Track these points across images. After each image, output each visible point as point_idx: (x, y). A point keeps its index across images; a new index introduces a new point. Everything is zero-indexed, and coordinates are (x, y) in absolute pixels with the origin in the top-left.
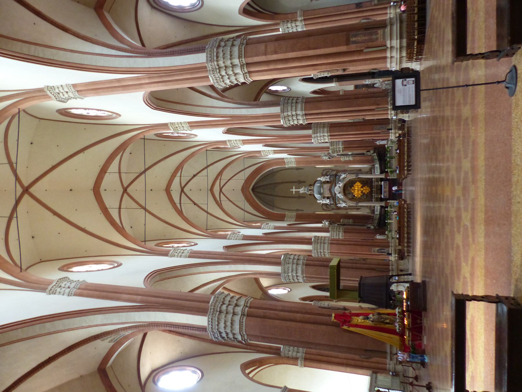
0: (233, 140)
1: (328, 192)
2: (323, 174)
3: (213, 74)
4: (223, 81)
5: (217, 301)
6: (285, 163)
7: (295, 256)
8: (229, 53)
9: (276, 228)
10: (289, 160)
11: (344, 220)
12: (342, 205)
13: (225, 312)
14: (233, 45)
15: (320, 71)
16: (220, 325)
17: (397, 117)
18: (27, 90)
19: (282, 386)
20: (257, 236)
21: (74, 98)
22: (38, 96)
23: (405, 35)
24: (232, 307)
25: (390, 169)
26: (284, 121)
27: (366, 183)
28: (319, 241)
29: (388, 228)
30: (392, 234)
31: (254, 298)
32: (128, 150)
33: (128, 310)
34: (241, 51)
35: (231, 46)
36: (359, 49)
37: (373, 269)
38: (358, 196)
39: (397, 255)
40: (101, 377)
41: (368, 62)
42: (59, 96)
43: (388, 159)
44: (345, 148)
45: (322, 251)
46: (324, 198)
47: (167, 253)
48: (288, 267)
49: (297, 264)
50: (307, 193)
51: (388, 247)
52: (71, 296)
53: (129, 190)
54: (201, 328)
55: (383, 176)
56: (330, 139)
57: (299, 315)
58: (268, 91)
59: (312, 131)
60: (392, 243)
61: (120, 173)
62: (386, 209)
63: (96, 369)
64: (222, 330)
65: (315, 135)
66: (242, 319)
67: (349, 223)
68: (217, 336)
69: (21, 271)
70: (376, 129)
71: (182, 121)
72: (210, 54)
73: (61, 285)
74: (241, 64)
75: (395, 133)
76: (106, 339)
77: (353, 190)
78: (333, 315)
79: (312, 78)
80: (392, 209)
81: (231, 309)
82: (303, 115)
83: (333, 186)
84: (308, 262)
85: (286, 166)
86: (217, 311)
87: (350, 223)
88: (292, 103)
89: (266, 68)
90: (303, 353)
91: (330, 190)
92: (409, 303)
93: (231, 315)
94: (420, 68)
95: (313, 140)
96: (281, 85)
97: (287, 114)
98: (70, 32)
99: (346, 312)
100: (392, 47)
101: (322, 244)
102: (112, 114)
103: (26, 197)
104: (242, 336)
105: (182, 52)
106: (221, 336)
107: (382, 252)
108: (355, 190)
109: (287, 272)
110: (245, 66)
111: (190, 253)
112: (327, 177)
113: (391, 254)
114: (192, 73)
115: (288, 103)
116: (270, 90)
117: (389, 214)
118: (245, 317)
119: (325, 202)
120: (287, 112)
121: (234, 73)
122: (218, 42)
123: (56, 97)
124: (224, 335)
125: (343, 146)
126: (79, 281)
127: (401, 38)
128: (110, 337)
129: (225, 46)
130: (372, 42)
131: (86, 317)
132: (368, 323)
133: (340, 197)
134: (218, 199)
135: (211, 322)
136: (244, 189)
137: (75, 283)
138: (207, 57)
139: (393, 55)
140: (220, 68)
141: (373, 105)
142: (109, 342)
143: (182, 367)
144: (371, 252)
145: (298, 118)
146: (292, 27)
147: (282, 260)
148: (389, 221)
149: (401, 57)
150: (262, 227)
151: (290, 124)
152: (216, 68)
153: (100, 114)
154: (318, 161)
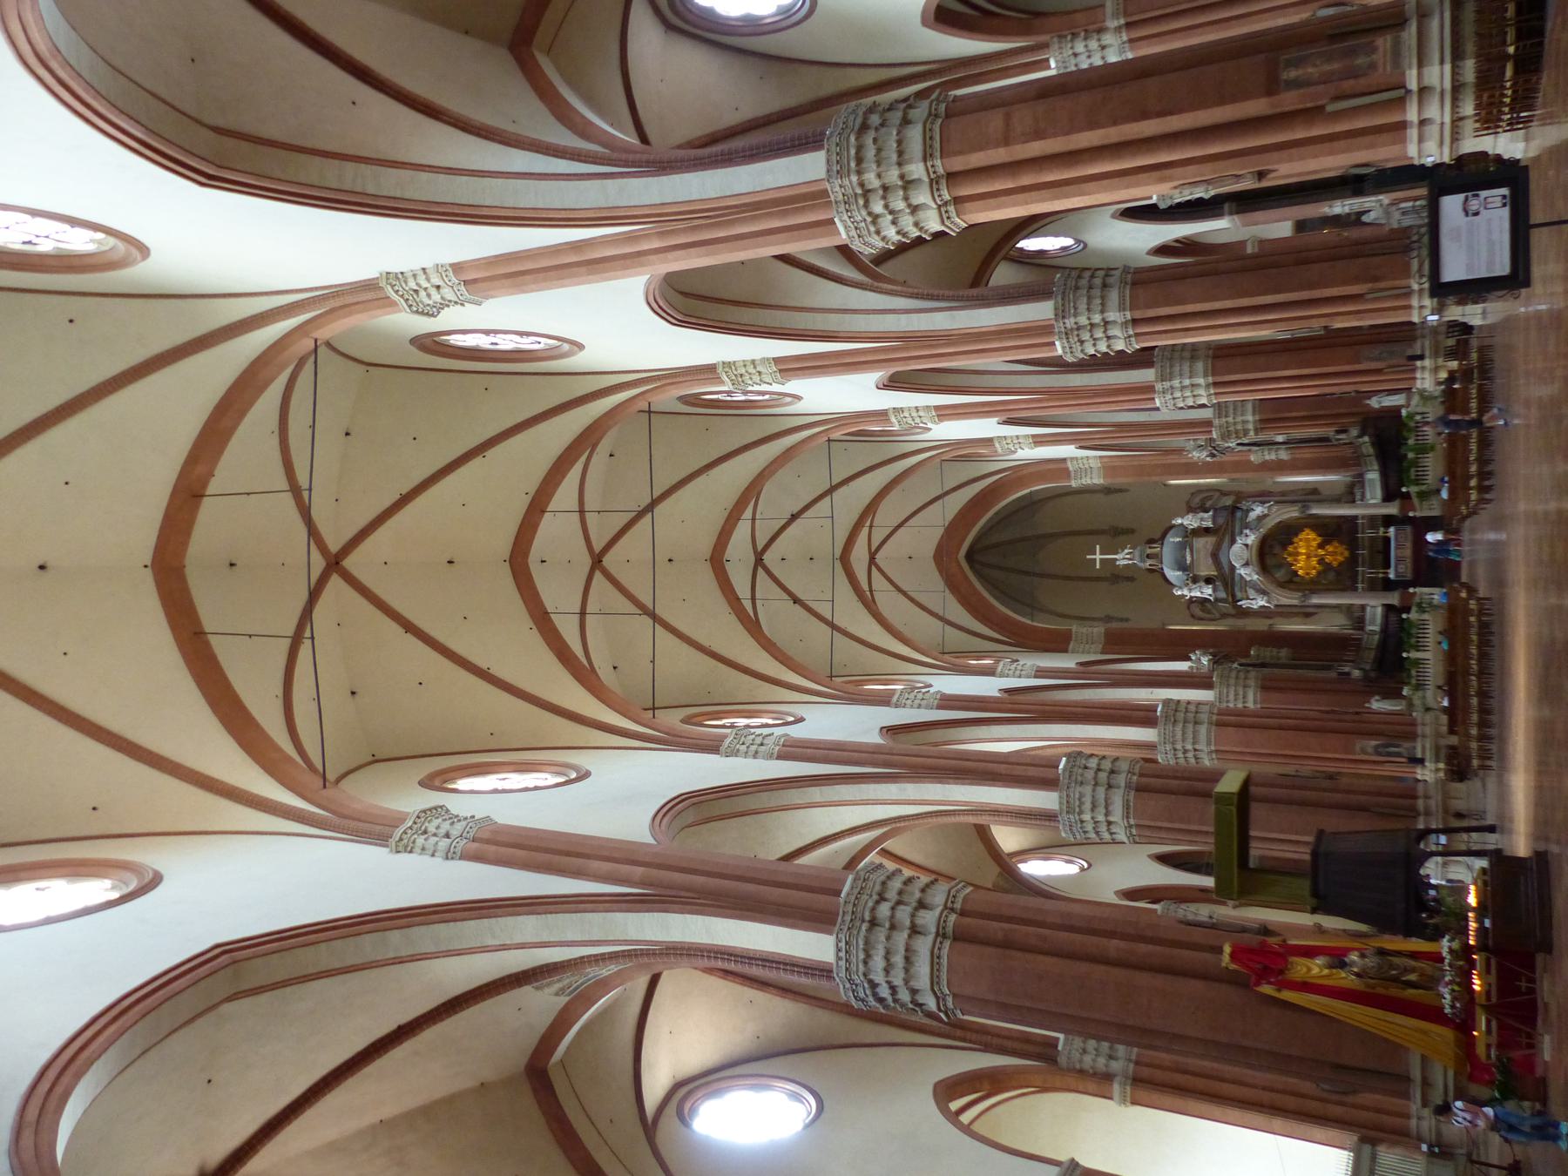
0: (909, 409)
1: (1210, 561)
2: (1193, 505)
3: (847, 211)
4: (878, 232)
5: (862, 888)
7: (1103, 762)
8: (895, 145)
9: (1040, 673)
10: (1081, 465)
11: (1262, 649)
12: (1253, 602)
13: (887, 925)
14: (906, 122)
15: (1181, 182)
16: (871, 963)
17: (1441, 317)
18: (336, 286)
19: (1063, 1157)
20: (984, 697)
21: (456, 303)
22: (363, 302)
23: (1470, 47)
24: (909, 909)
25: (1417, 484)
26: (1066, 345)
27: (1331, 531)
28: (1181, 716)
29: (1409, 676)
30: (1424, 697)
31: (976, 886)
32: (604, 447)
33: (607, 905)
34: (931, 138)
35: (901, 125)
36: (1309, 105)
37: (1362, 809)
39: (1442, 765)
40: (535, 1091)
41: (1342, 144)
42: (418, 300)
43: (1411, 455)
44: (1260, 420)
45: (1189, 747)
46: (1195, 580)
47: (716, 743)
48: (1081, 796)
49: (1110, 786)
50: (1141, 565)
51: (1412, 737)
52: (452, 858)
53: (607, 561)
54: (816, 969)
55: (1392, 509)
56: (1216, 394)
57: (1115, 942)
58: (1016, 254)
59: (1157, 372)
61: (582, 512)
62: (1404, 616)
63: (522, 1068)
64: (879, 977)
65: (1167, 384)
66: (939, 949)
67: (1279, 659)
68: (862, 995)
69: (325, 787)
71: (757, 356)
72: (838, 154)
73: (426, 827)
74: (933, 176)
75: (1436, 369)
76: (549, 985)
77: (1290, 555)
78: (1227, 949)
79: (1154, 206)
80: (1426, 616)
81: (904, 914)
82: (1125, 324)
84: (1145, 780)
85: (1074, 484)
86: (863, 921)
87: (1284, 661)
88: (1091, 288)
89: (1010, 185)
90: (1130, 1060)
91: (1215, 556)
92: (1487, 923)
93: (905, 934)
94: (1526, 151)
95: (1157, 401)
96: (1056, 235)
97: (1076, 323)
98: (445, 118)
99: (1272, 940)
100: (1423, 91)
101: (1190, 727)
102: (560, 343)
103: (335, 581)
104: (937, 998)
105: (754, 152)
106: (875, 995)
107: (1389, 754)
108: (1298, 554)
109: (1077, 810)
110: (944, 182)
111: (783, 746)
112: (1206, 515)
113: (1421, 761)
114: (785, 213)
115: (1077, 288)
116: (1021, 249)
117: (1414, 631)
118: (949, 942)
119: (1198, 594)
120: (1075, 315)
121: (909, 206)
122: (861, 113)
123: (410, 302)
124: (884, 992)
125: (1257, 417)
126: (473, 817)
127: (1457, 56)
128: (559, 981)
129: (882, 125)
130: (1356, 77)
131: (493, 920)
132: (1344, 979)
133: (1248, 579)
134: (865, 587)
135: (845, 951)
136: (942, 555)
137: (464, 823)
138: (828, 161)
139: (1426, 115)
140: (867, 193)
141: (1356, 280)
142: (557, 994)
143: (760, 1081)
144: (1355, 754)
145: (1110, 333)
146: (1089, 51)
147: (1060, 772)
148: (1414, 655)
149: (1457, 121)
150: (999, 669)
151: (1086, 354)
152: (856, 194)
153: (526, 344)
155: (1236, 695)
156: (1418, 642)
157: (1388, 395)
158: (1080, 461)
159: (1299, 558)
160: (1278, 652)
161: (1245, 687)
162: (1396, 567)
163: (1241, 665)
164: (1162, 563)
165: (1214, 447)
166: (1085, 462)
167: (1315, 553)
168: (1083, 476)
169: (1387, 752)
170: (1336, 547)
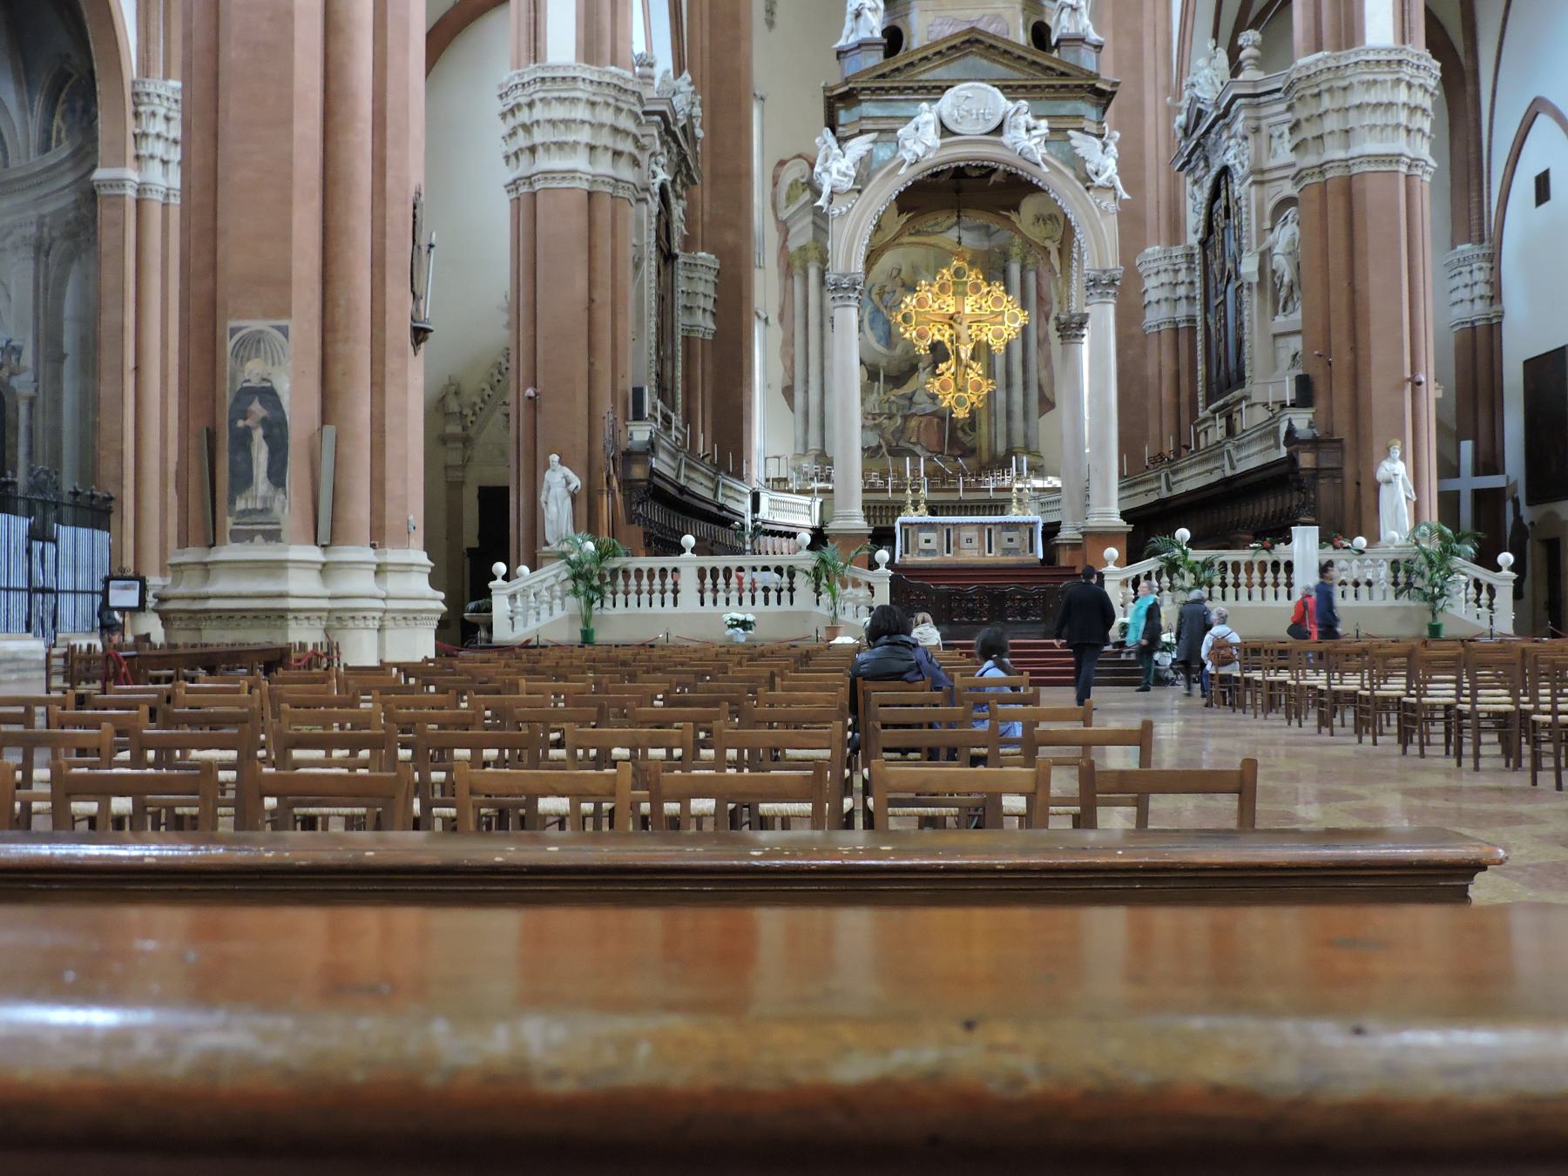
11: (711, 277)
38: (906, 318)
60: (380, 570)
67: (688, 309)
77: (958, 273)
83: (1000, 71)
87: (682, 319)
108: (960, 294)
155: (567, 122)
157: (1407, 498)
159: (950, 300)
161: (592, 148)
162: (930, 527)
165: (1225, 114)
167: (964, 336)
169: (247, 432)
170: (978, 387)
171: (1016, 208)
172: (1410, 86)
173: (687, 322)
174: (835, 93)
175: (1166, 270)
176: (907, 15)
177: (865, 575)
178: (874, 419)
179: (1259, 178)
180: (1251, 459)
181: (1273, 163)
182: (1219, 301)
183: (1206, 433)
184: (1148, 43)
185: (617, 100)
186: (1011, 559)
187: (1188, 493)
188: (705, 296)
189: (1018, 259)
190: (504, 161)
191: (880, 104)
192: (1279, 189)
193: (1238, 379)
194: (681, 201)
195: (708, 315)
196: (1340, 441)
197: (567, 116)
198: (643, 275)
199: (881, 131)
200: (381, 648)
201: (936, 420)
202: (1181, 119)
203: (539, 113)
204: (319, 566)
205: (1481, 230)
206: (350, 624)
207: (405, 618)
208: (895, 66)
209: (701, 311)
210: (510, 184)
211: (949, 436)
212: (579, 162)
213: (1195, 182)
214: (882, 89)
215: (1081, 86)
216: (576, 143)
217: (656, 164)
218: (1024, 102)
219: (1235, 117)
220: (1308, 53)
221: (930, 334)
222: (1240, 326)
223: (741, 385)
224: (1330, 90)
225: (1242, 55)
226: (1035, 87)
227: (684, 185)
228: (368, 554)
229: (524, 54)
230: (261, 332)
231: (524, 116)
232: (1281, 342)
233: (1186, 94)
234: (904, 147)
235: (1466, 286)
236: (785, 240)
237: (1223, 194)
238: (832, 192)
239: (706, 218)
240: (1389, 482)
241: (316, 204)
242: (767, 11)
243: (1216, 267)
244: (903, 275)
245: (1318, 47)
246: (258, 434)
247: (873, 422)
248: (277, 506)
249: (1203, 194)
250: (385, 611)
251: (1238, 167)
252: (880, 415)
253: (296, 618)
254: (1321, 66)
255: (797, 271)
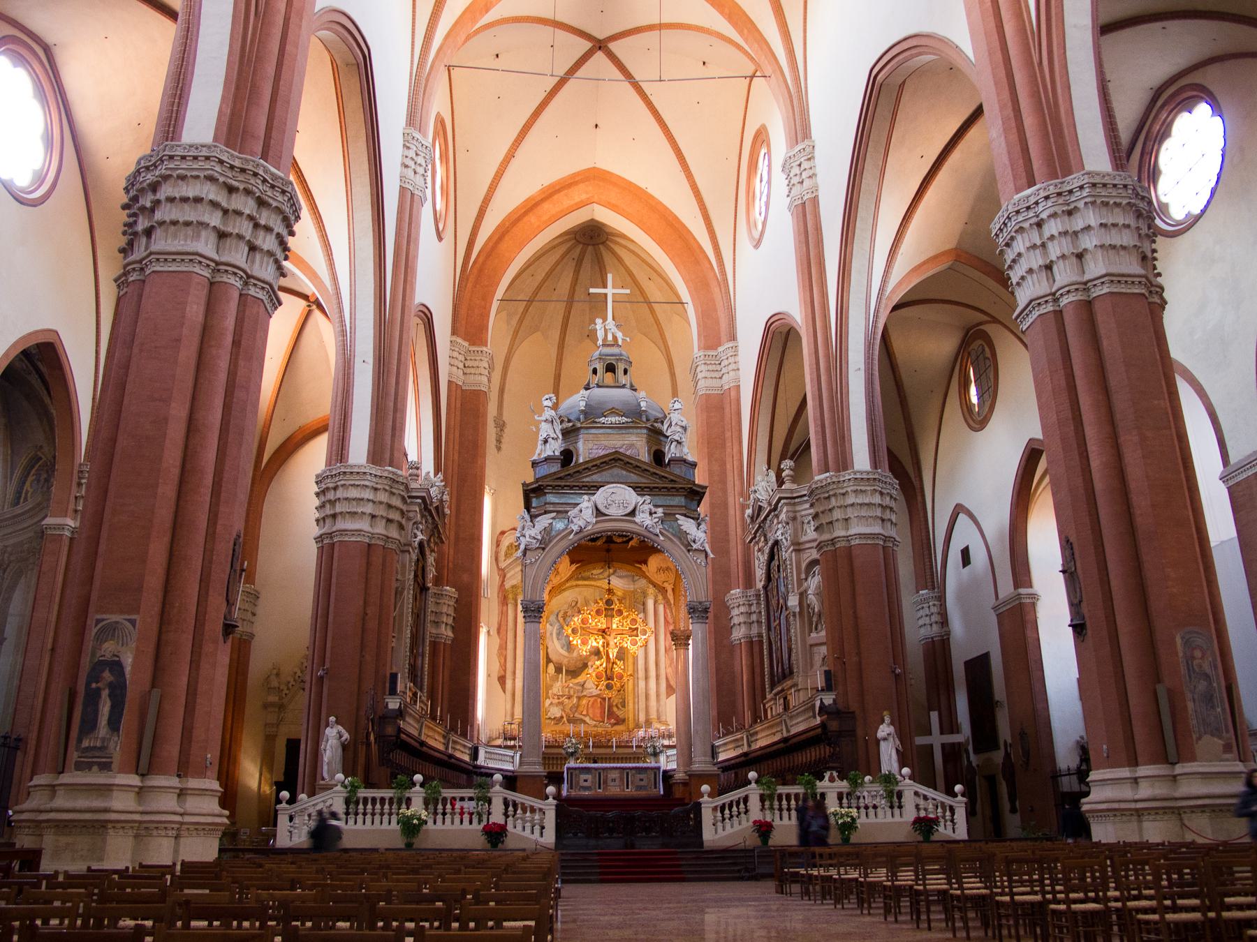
6: (714, 347)
9: (409, 201)
10: (725, 363)
11: (452, 603)
56: (1059, 314)
60: (182, 793)
67: (437, 624)
70: (1186, 643)
83: (634, 478)
87: (431, 629)
91: (615, 460)
154: (724, 491)
156: (444, 805)
158: (731, 360)
159: (603, 620)
160: (446, 624)
163: (421, 544)
164: (598, 386)
165: (775, 509)
166: (731, 367)
167: (612, 643)
168: (710, 368)
169: (99, 689)
171: (645, 562)
172: (881, 494)
173: (434, 631)
174: (529, 488)
175: (744, 604)
176: (576, 443)
177: (537, 803)
178: (559, 699)
179: (797, 548)
180: (799, 726)
181: (804, 539)
182: (776, 623)
183: (771, 709)
184: (729, 466)
185: (391, 487)
186: (643, 793)
187: (761, 748)
188: (447, 615)
189: (652, 597)
190: (315, 523)
191: (559, 496)
192: (809, 554)
193: (788, 673)
194: (433, 554)
195: (448, 627)
196: (853, 712)
197: (358, 496)
198: (403, 601)
199: (558, 512)
200: (176, 851)
201: (599, 700)
202: (749, 511)
203: (340, 493)
204: (137, 789)
205: (933, 582)
206: (155, 833)
207: (196, 829)
208: (567, 473)
209: (444, 626)
210: (318, 538)
211: (608, 711)
212: (364, 525)
213: (759, 550)
214: (559, 486)
215: (684, 488)
216: (363, 513)
217: (417, 529)
218: (648, 497)
219: (781, 511)
220: (820, 473)
221: (590, 642)
222: (789, 640)
223: (469, 674)
224: (835, 495)
225: (784, 474)
226: (655, 488)
227: (436, 543)
228: (174, 782)
229: (334, 458)
230: (117, 623)
231: (331, 496)
232: (815, 649)
233: (751, 496)
234: (572, 522)
235: (927, 616)
236: (503, 581)
237: (776, 558)
238: (525, 549)
239: (451, 565)
240: (885, 739)
241: (166, 539)
242: (497, 441)
243: (773, 602)
244: (579, 605)
245: (827, 471)
246: (105, 693)
247: (557, 701)
248: (112, 745)
249: (763, 558)
250: (182, 823)
251: (784, 540)
252: (562, 696)
253: (114, 827)
254: (829, 481)
255: (511, 601)
